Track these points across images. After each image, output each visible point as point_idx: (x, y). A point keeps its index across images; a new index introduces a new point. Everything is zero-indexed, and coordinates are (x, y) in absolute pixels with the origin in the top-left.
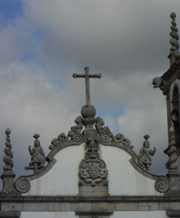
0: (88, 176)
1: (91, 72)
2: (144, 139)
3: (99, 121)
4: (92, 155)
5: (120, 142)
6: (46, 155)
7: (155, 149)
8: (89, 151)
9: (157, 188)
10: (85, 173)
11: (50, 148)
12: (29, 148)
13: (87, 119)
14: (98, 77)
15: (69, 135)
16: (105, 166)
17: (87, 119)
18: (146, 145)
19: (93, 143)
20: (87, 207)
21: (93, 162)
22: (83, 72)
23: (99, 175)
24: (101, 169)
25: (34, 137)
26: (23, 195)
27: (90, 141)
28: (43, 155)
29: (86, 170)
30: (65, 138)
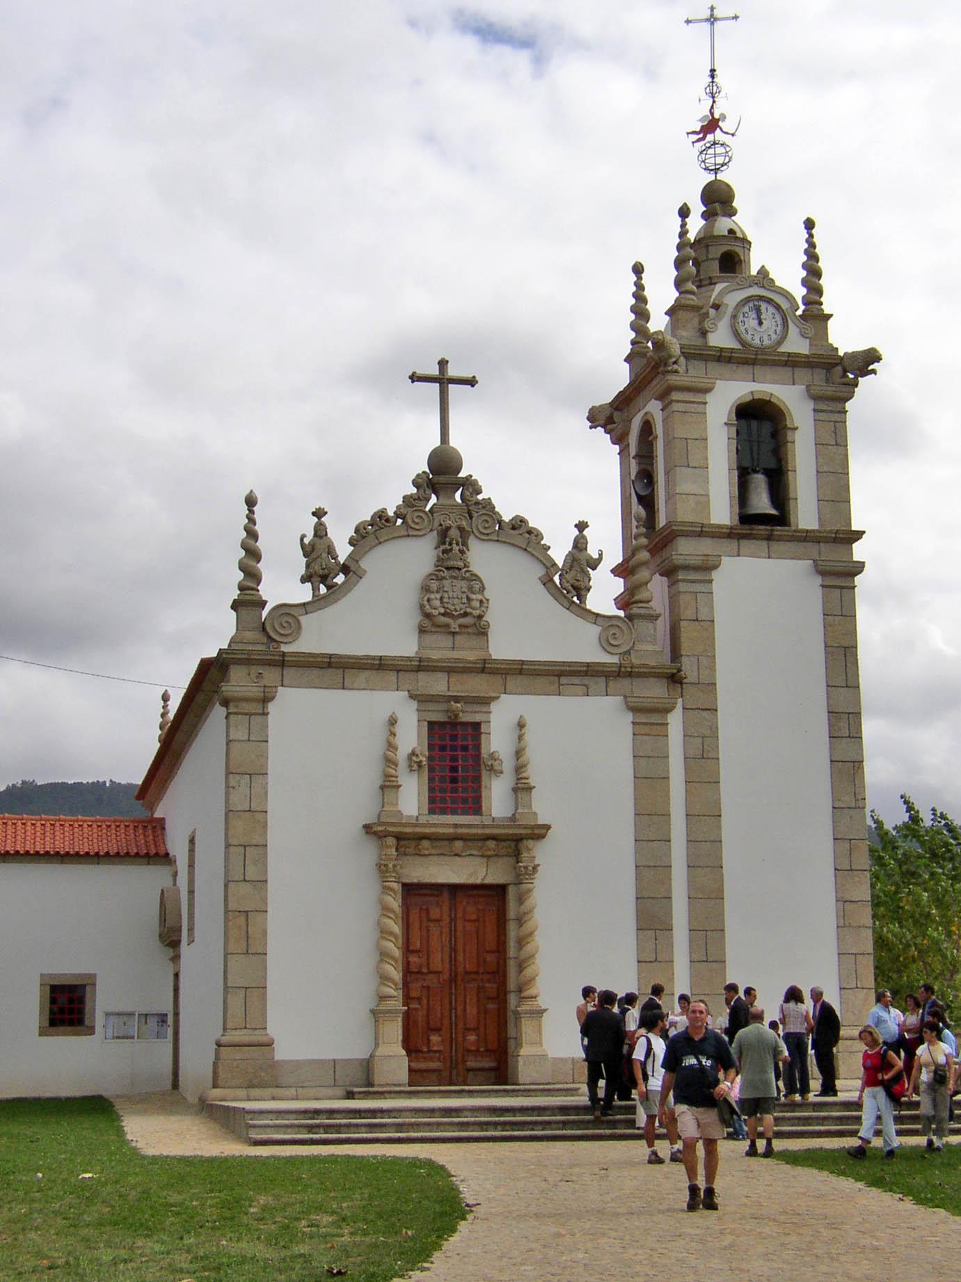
0: (442, 611)
1: (452, 372)
2: (576, 532)
3: (470, 486)
4: (450, 564)
5: (522, 535)
6: (342, 560)
7: (601, 555)
8: (444, 552)
9: (606, 644)
10: (437, 603)
11: (351, 543)
12: (302, 540)
13: (442, 479)
14: (472, 382)
15: (397, 515)
16: (482, 589)
17: (442, 479)
18: (580, 544)
19: (454, 533)
20: (438, 684)
21: (455, 578)
22: (434, 371)
23: (469, 610)
24: (474, 596)
25: (314, 514)
26: (284, 648)
27: (448, 529)
28: (335, 558)
29: (438, 596)
30: (387, 520)
